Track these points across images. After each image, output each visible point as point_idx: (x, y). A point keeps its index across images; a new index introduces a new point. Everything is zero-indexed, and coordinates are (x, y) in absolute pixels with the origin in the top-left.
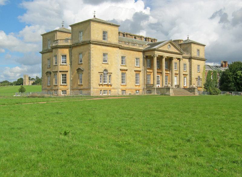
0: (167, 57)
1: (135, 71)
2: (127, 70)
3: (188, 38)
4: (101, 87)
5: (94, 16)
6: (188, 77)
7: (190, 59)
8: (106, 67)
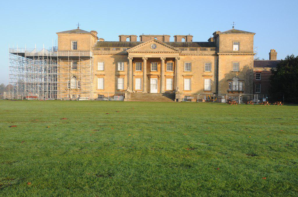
0: (148, 58)
3: (233, 27)
5: (78, 27)
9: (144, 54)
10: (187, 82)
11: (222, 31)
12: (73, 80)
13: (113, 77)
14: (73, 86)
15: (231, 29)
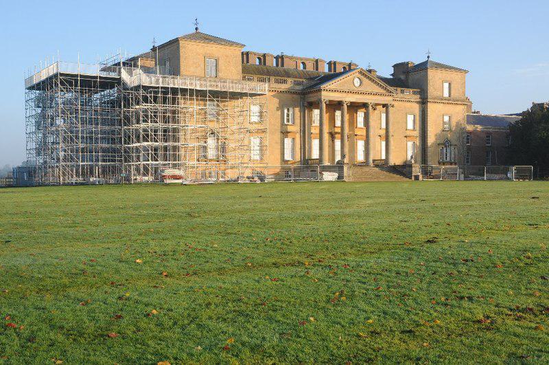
9: (344, 95)
12: (211, 142)
13: (278, 136)
14: (211, 153)
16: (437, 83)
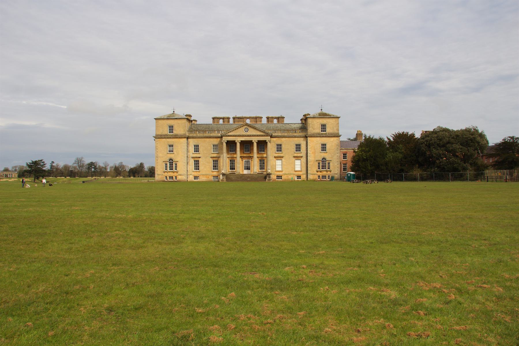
1: (211, 158)
2: (200, 157)
4: (166, 174)
6: (304, 160)
7: (306, 137)
8: (172, 156)
9: (238, 138)
10: (279, 162)
11: (311, 116)
15: (320, 111)
16: (314, 126)
